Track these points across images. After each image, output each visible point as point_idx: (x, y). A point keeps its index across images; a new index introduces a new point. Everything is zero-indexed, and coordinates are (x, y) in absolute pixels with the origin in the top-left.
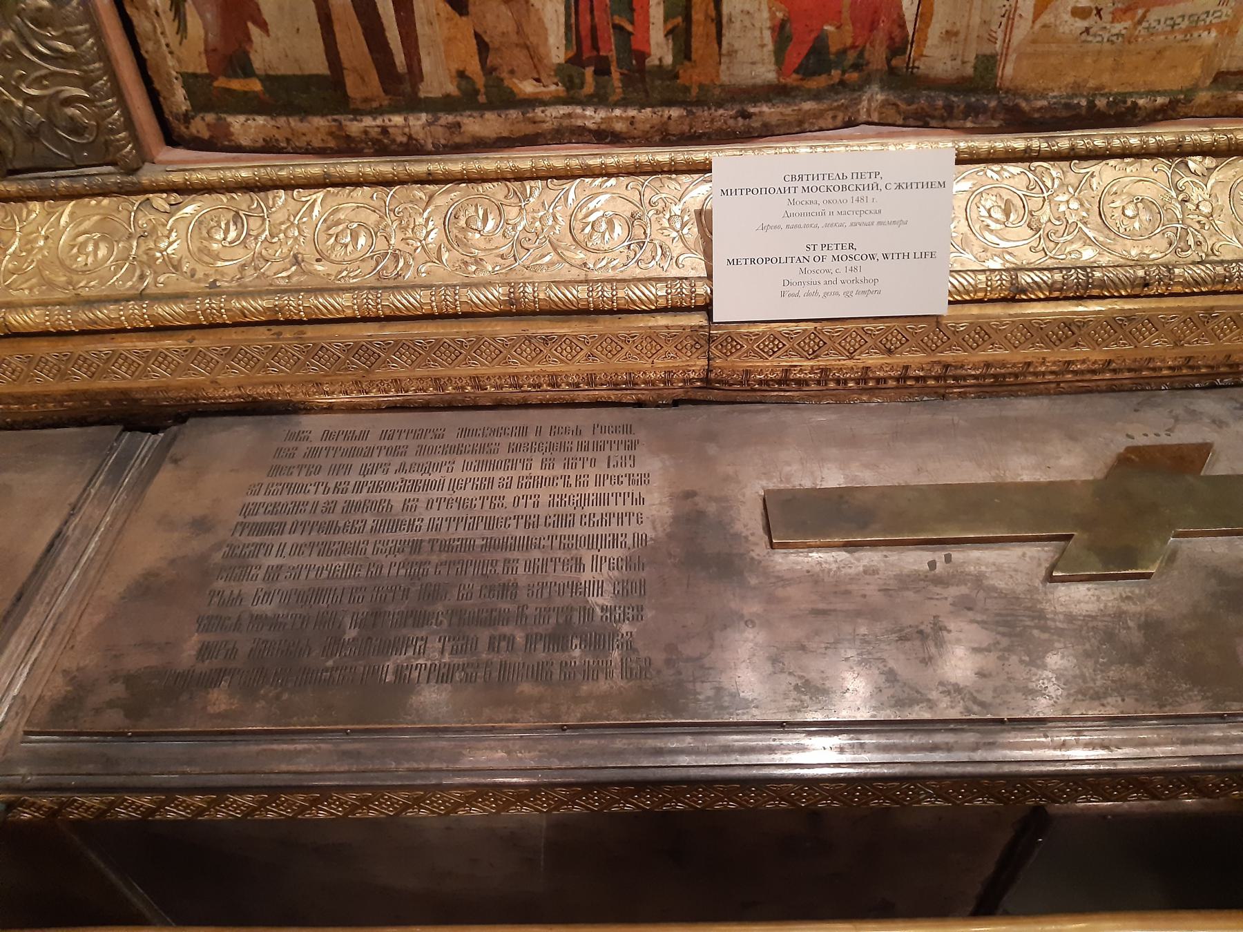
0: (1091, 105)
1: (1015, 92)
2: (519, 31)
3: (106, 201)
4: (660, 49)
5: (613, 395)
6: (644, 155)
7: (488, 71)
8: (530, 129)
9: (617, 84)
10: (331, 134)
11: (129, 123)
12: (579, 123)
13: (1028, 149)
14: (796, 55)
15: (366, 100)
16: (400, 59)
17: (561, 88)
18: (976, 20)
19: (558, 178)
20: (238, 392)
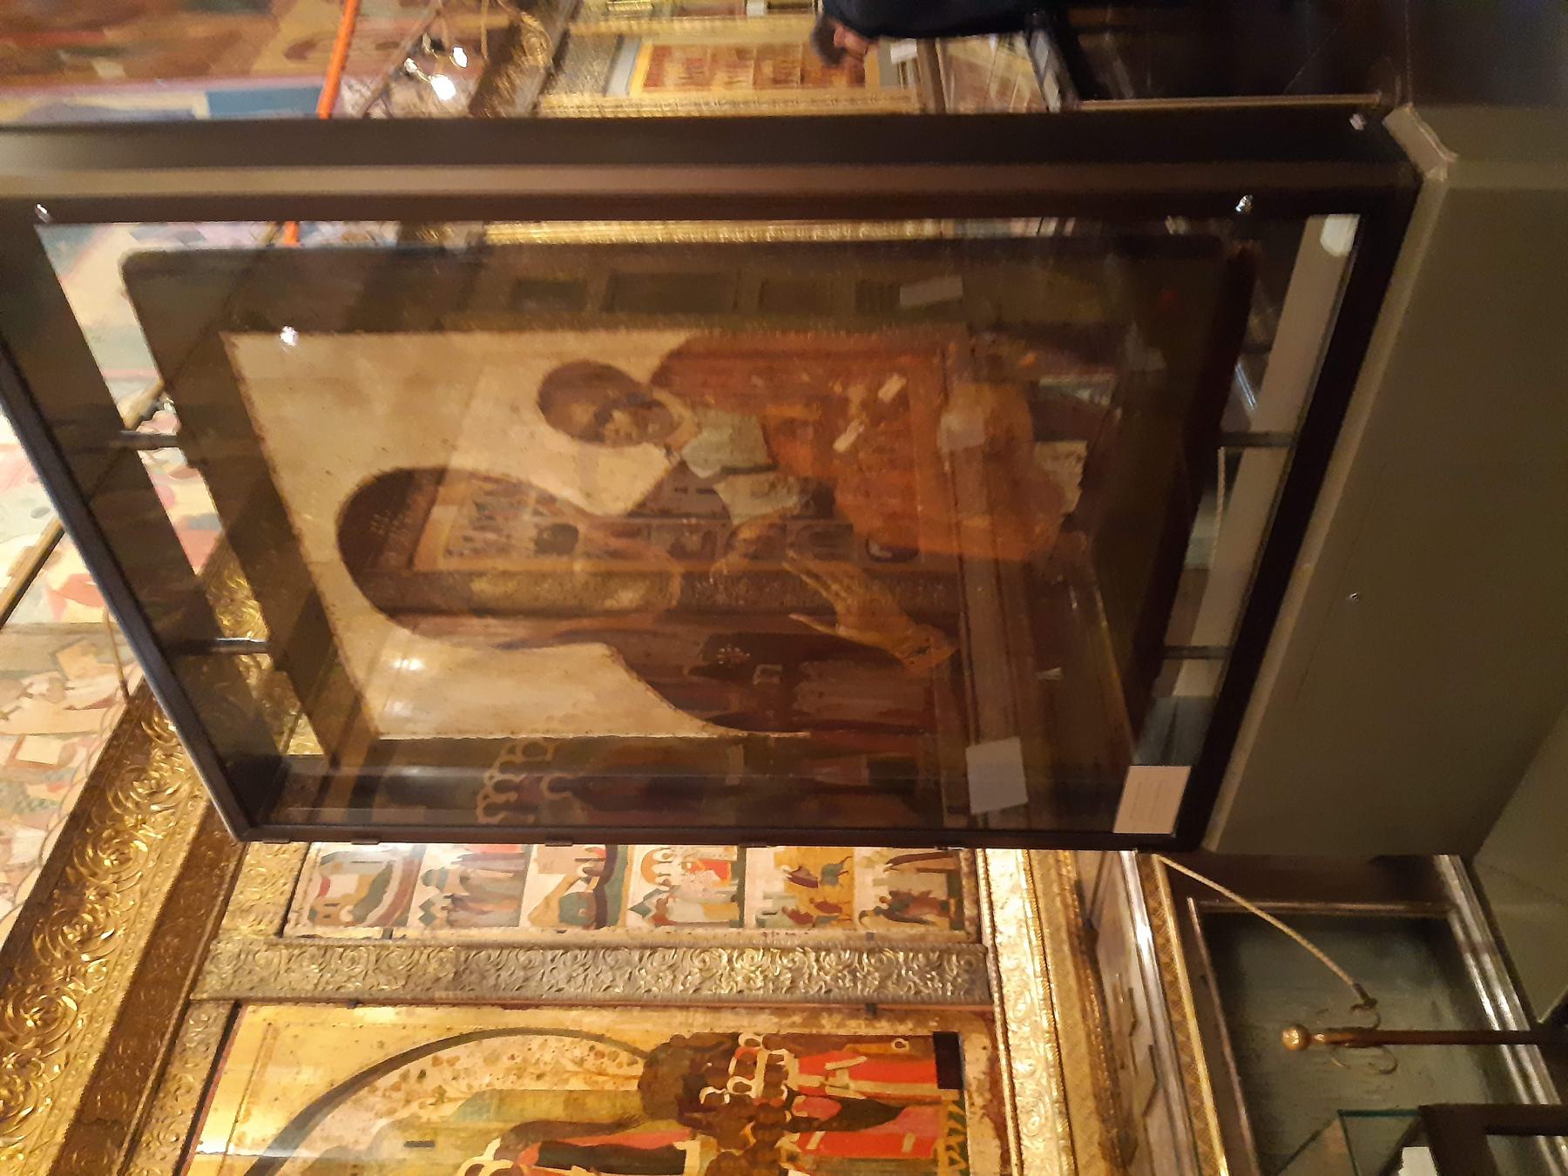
10: (968, 878)
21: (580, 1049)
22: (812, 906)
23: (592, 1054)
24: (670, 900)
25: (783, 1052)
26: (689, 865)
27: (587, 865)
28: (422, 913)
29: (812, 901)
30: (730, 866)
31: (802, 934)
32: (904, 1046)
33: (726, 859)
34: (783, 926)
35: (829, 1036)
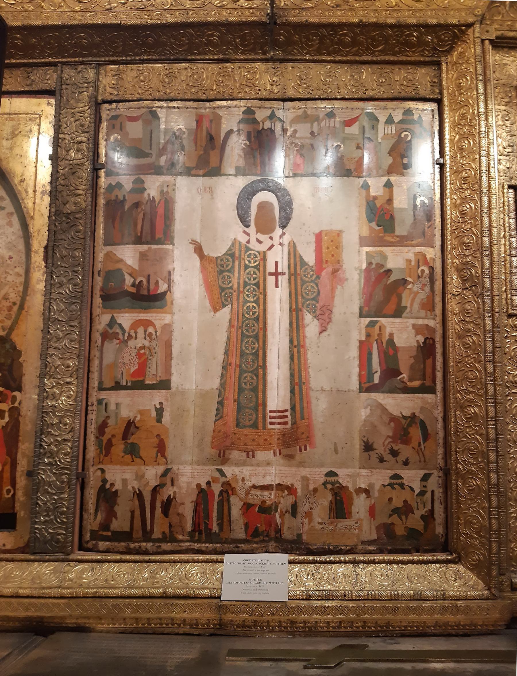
0: (329, 548)
1: (307, 544)
2: (180, 522)
3: (57, 563)
4: (215, 528)
5: (192, 631)
6: (209, 557)
7: (171, 532)
8: (179, 548)
9: (204, 537)
10: (126, 547)
11: (72, 542)
12: (193, 547)
13: (314, 560)
14: (250, 532)
15: (138, 538)
16: (149, 528)
17: (189, 538)
18: (295, 525)
19: (185, 562)
20: (76, 621)
21: (14, 297)
22: (110, 436)
23: (11, 304)
24: (118, 341)
25: (7, 419)
26: (142, 351)
27: (145, 283)
28: (114, 184)
29: (113, 436)
30: (141, 379)
31: (92, 428)
32: (8, 494)
33: (147, 376)
34: (97, 417)
35: (17, 447)
